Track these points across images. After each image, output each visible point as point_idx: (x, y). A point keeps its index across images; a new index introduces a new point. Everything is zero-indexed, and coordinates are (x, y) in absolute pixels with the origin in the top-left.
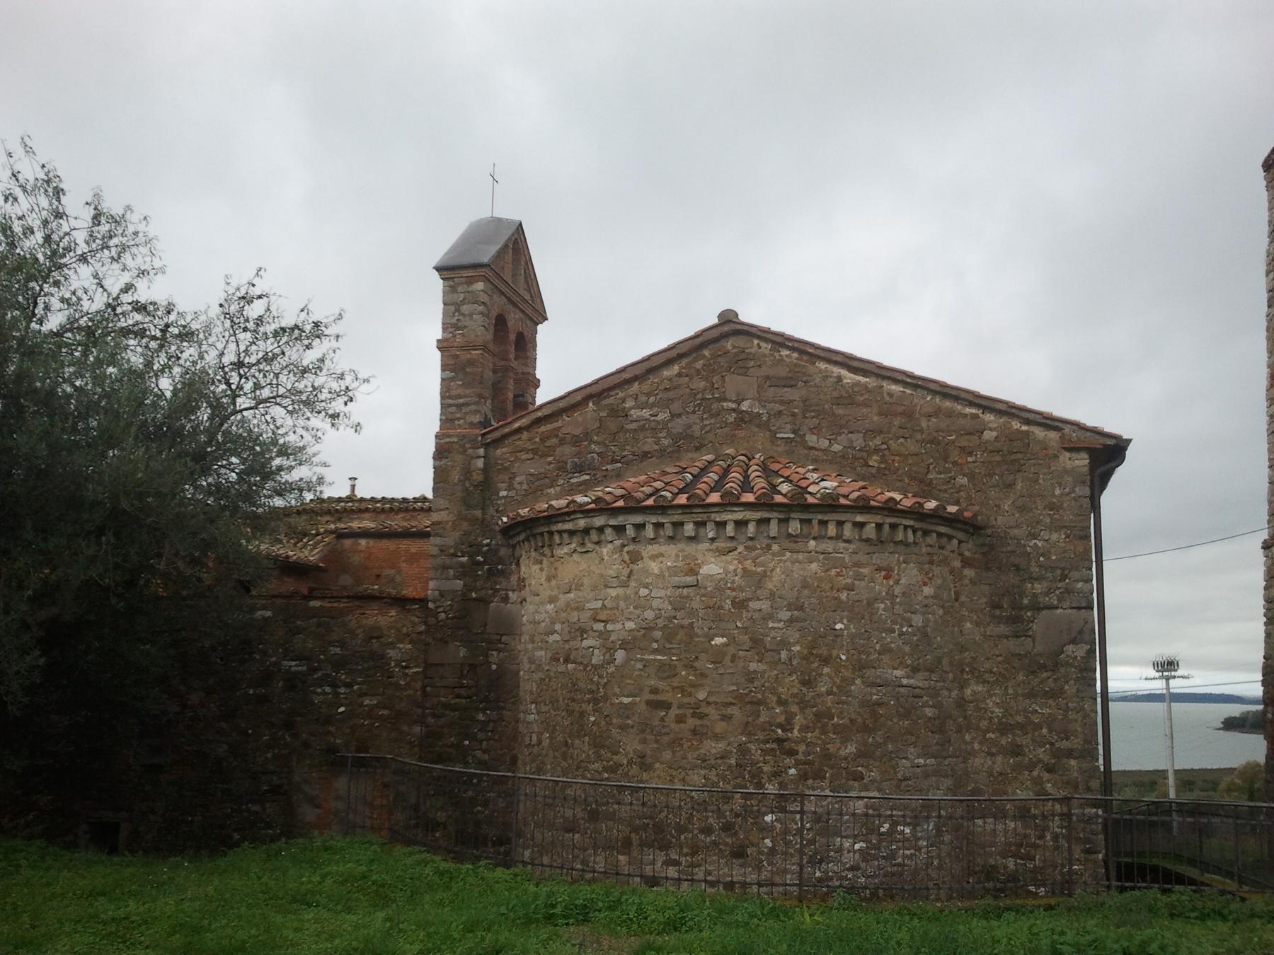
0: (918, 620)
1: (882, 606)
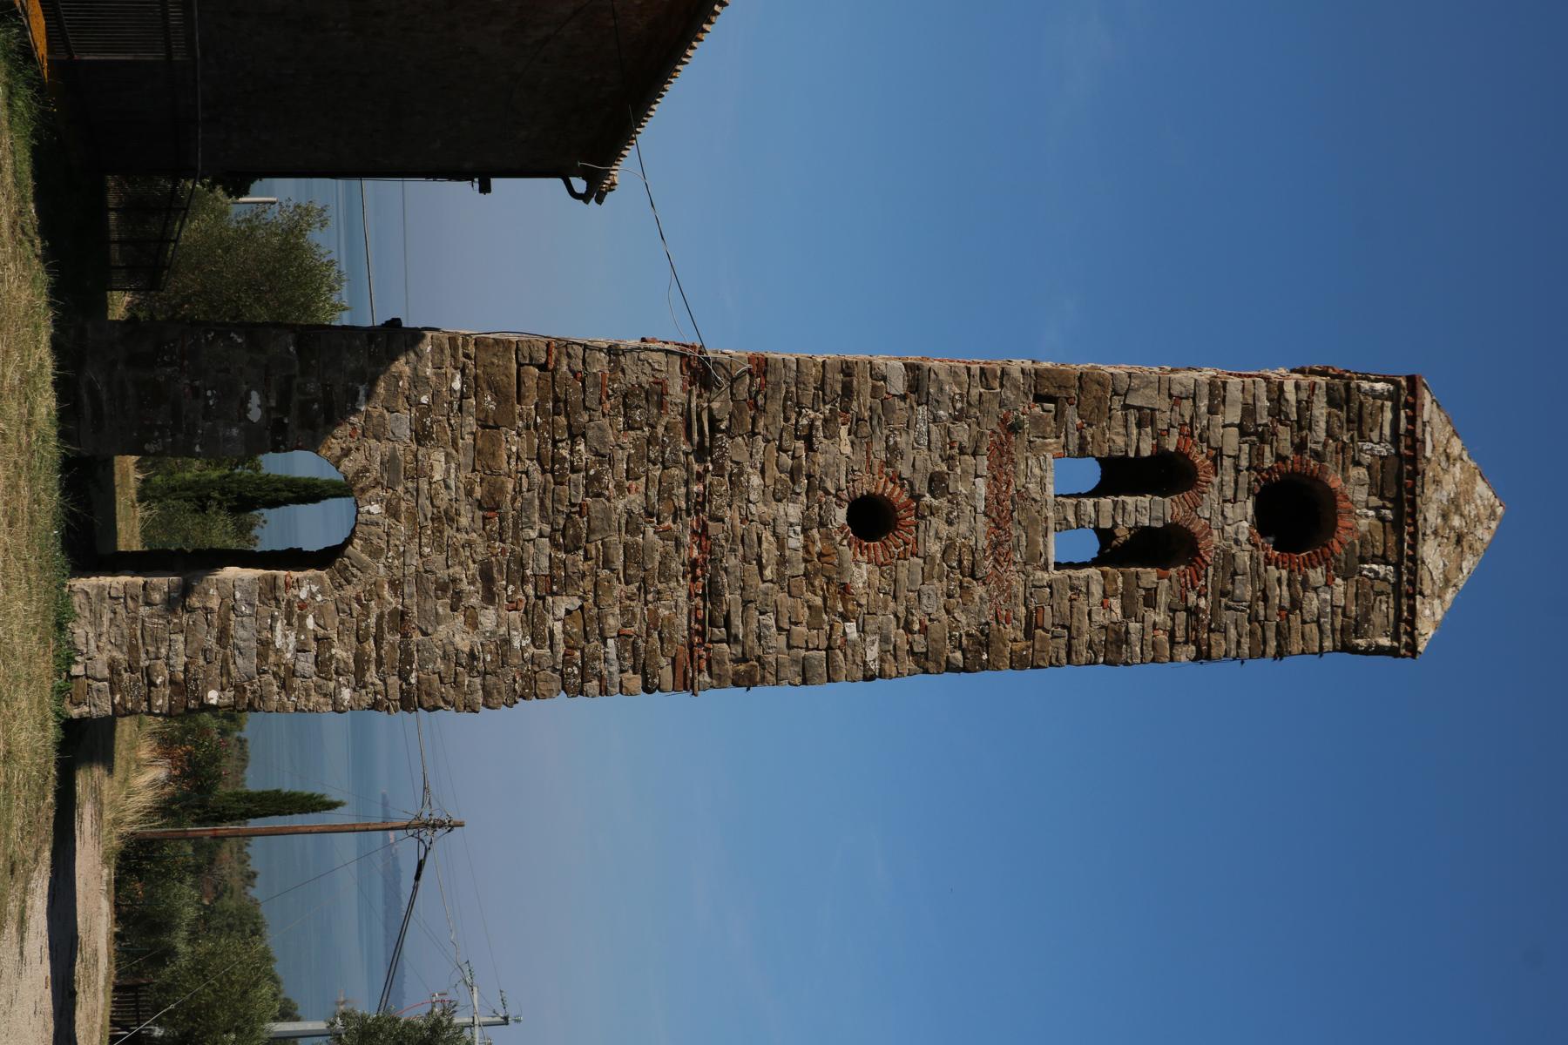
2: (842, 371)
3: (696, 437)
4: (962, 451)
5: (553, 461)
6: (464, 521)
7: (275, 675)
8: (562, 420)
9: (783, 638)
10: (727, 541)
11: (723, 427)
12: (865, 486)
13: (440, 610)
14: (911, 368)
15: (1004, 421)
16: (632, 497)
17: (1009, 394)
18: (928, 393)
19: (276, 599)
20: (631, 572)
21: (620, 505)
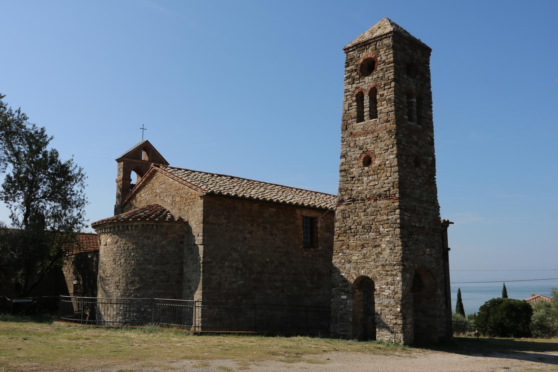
0: (159, 251)
1: (146, 247)
2: (341, 172)
3: (350, 202)
4: (355, 144)
5: (355, 233)
6: (365, 252)
7: (394, 295)
8: (348, 231)
9: (390, 178)
10: (370, 193)
11: (350, 196)
12: (361, 164)
13: (382, 257)
14: (341, 158)
15: (350, 136)
16: (361, 215)
17: (345, 136)
18: (345, 153)
19: (379, 294)
20: (375, 214)
21: (363, 217)
